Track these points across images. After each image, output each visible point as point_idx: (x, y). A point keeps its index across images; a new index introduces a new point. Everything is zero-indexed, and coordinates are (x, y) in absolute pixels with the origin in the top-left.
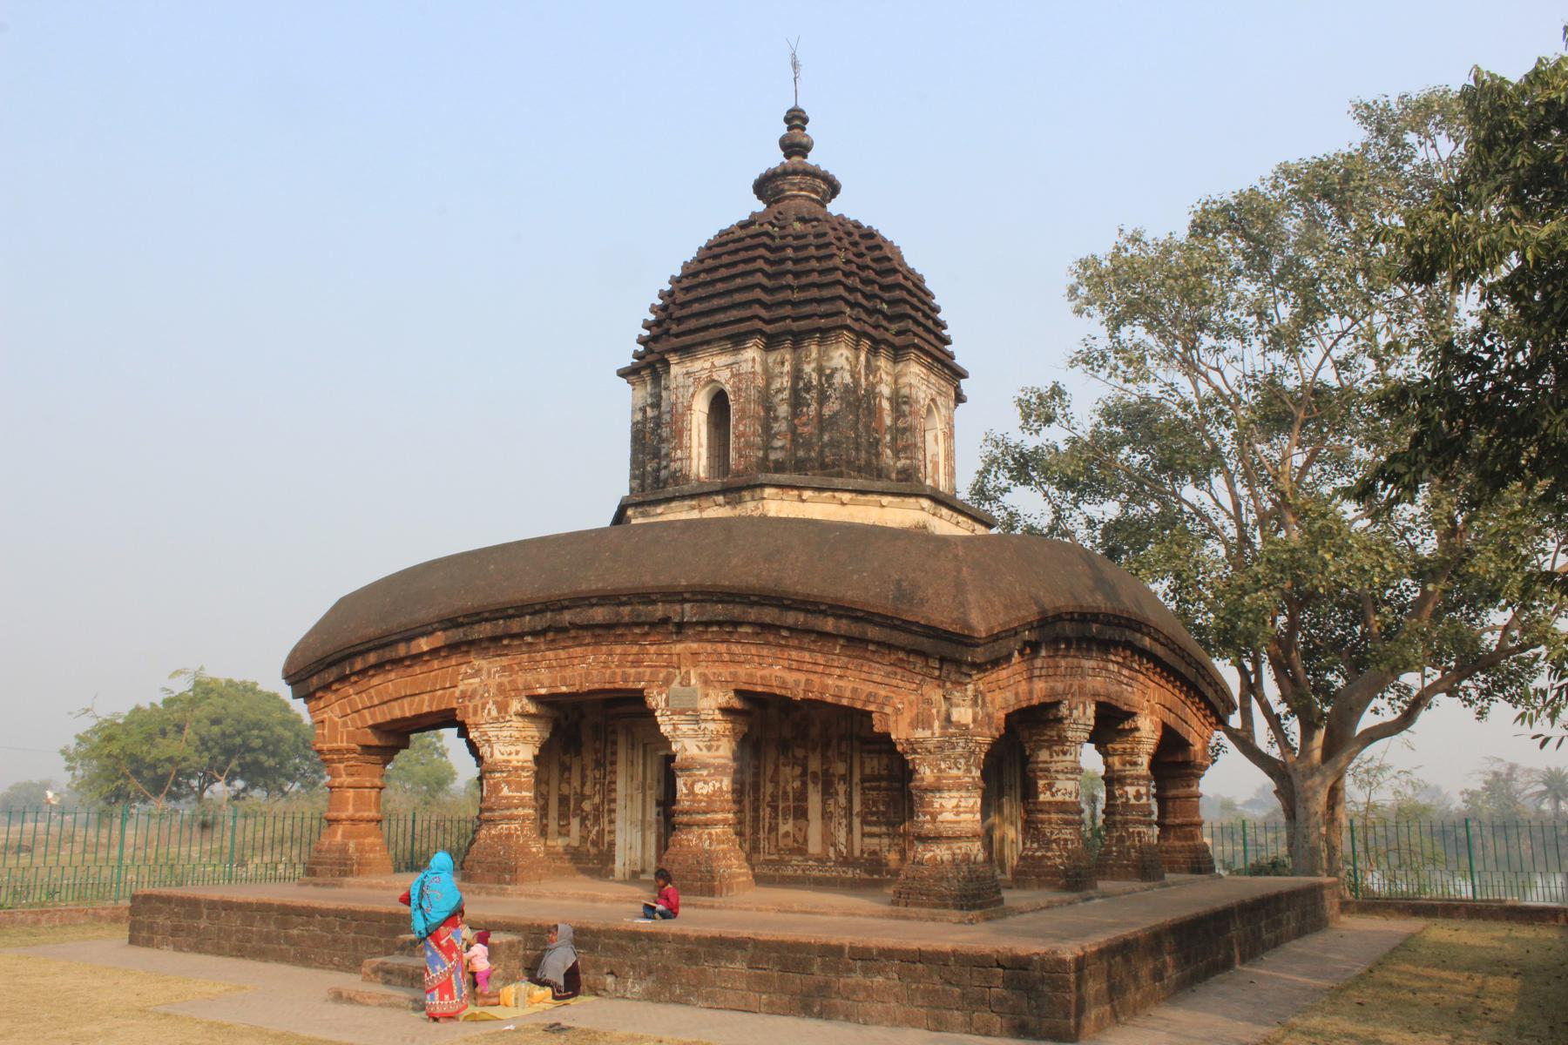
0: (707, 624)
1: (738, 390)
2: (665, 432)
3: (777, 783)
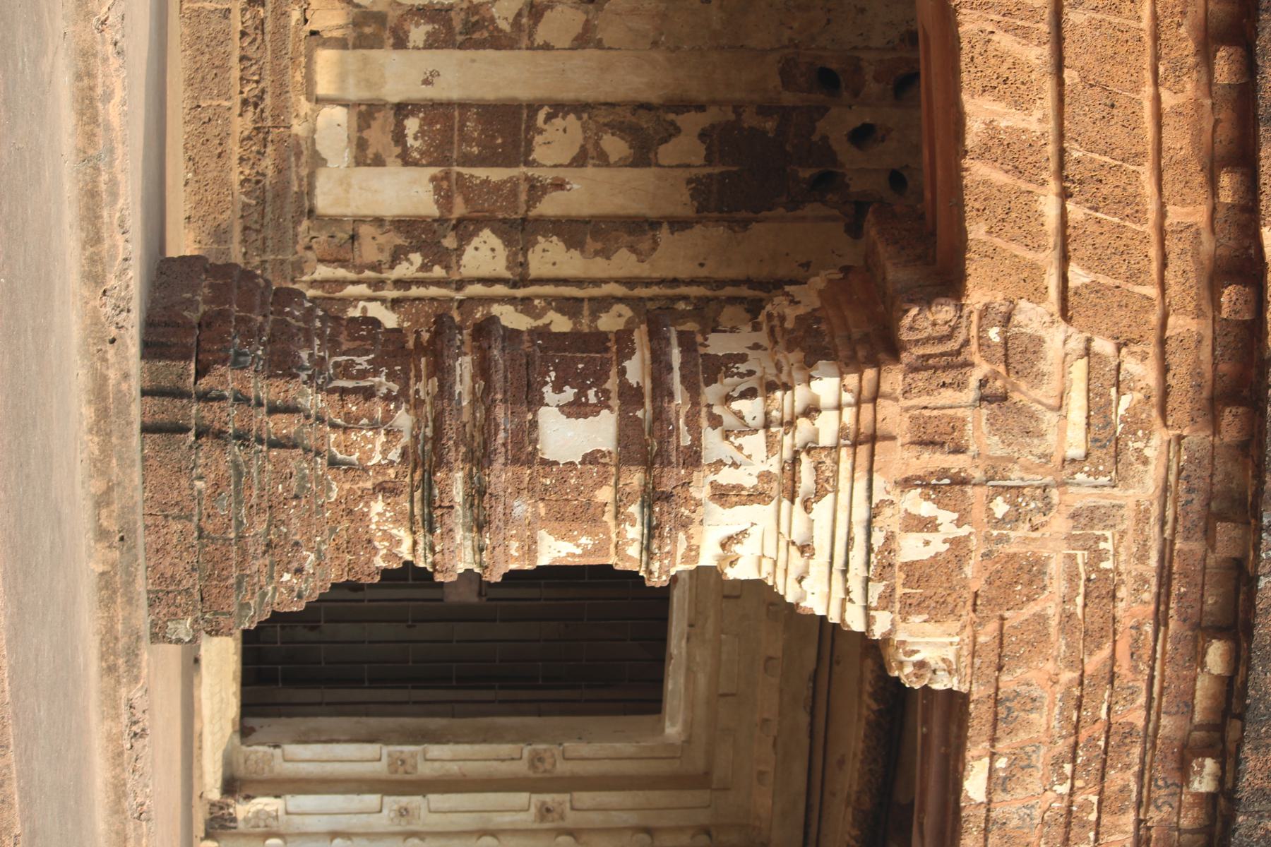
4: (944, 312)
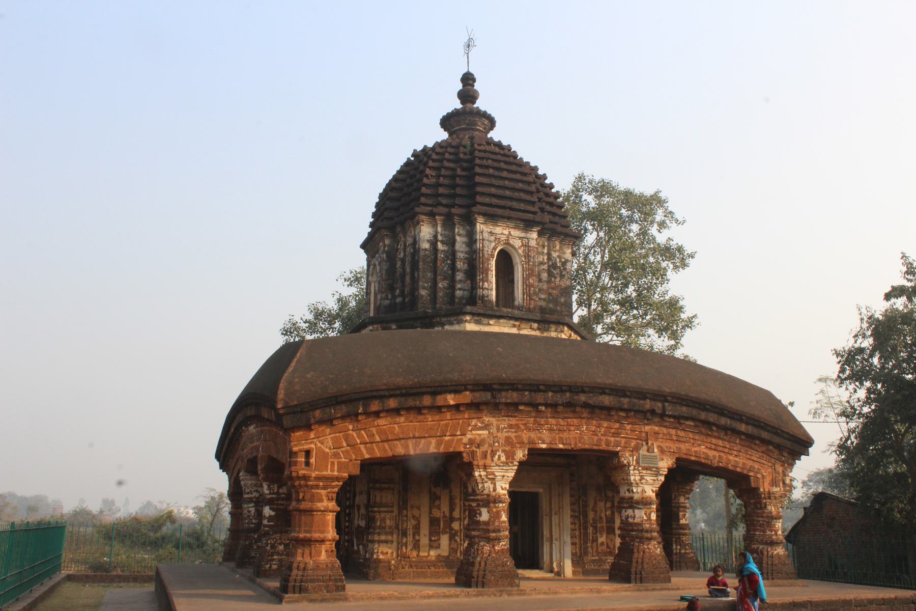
3: (596, 512)
4: (464, 454)
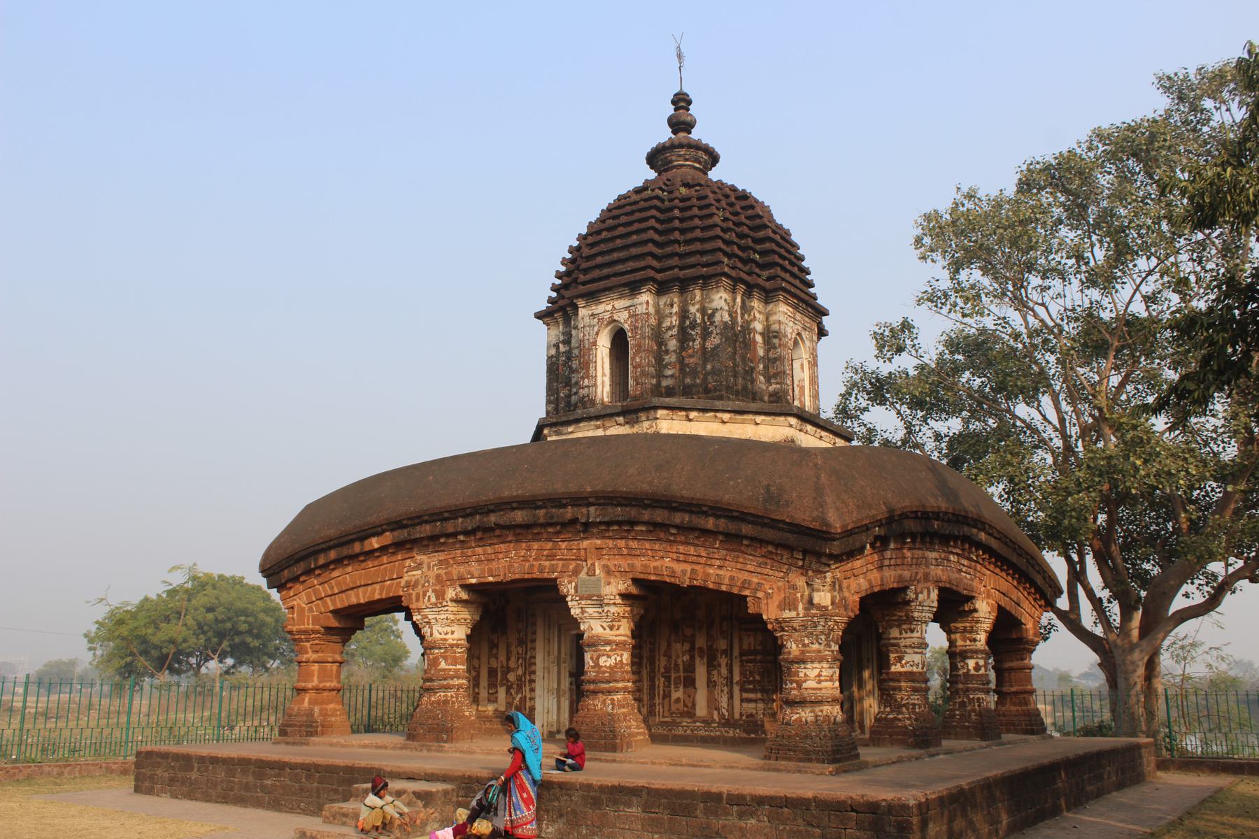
0: (609, 524)
1: (634, 328)
2: (575, 364)
3: (670, 657)
